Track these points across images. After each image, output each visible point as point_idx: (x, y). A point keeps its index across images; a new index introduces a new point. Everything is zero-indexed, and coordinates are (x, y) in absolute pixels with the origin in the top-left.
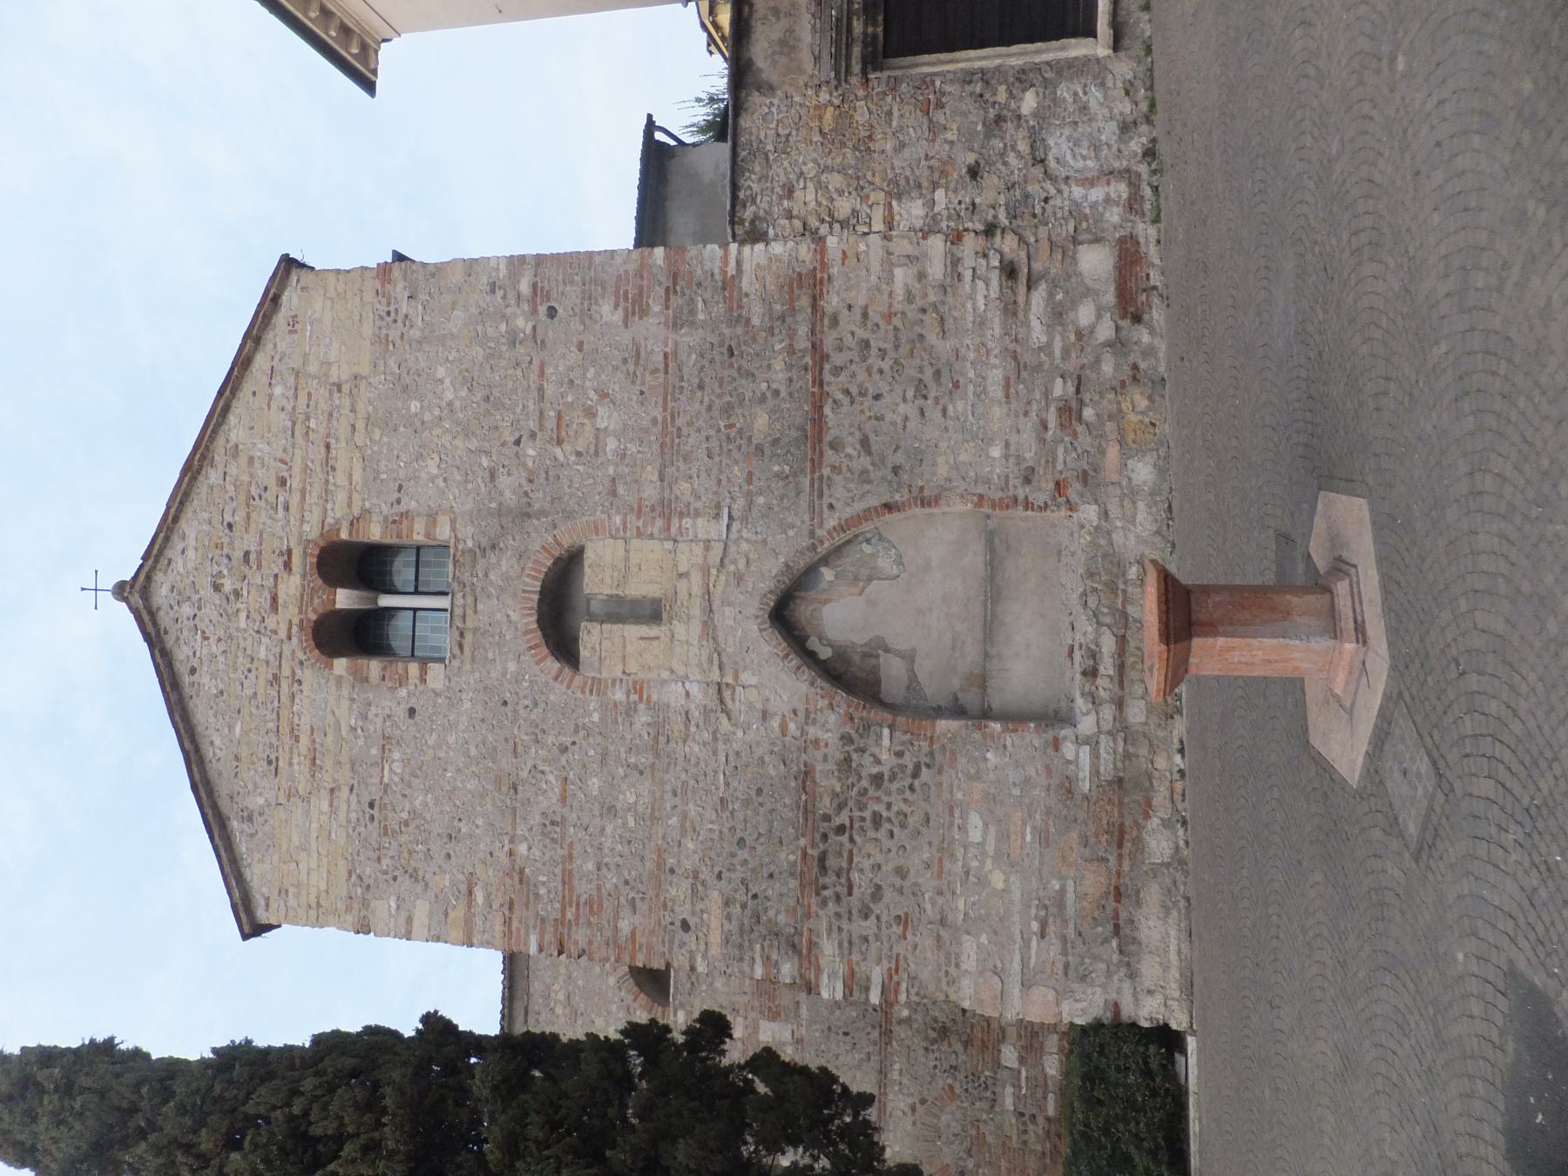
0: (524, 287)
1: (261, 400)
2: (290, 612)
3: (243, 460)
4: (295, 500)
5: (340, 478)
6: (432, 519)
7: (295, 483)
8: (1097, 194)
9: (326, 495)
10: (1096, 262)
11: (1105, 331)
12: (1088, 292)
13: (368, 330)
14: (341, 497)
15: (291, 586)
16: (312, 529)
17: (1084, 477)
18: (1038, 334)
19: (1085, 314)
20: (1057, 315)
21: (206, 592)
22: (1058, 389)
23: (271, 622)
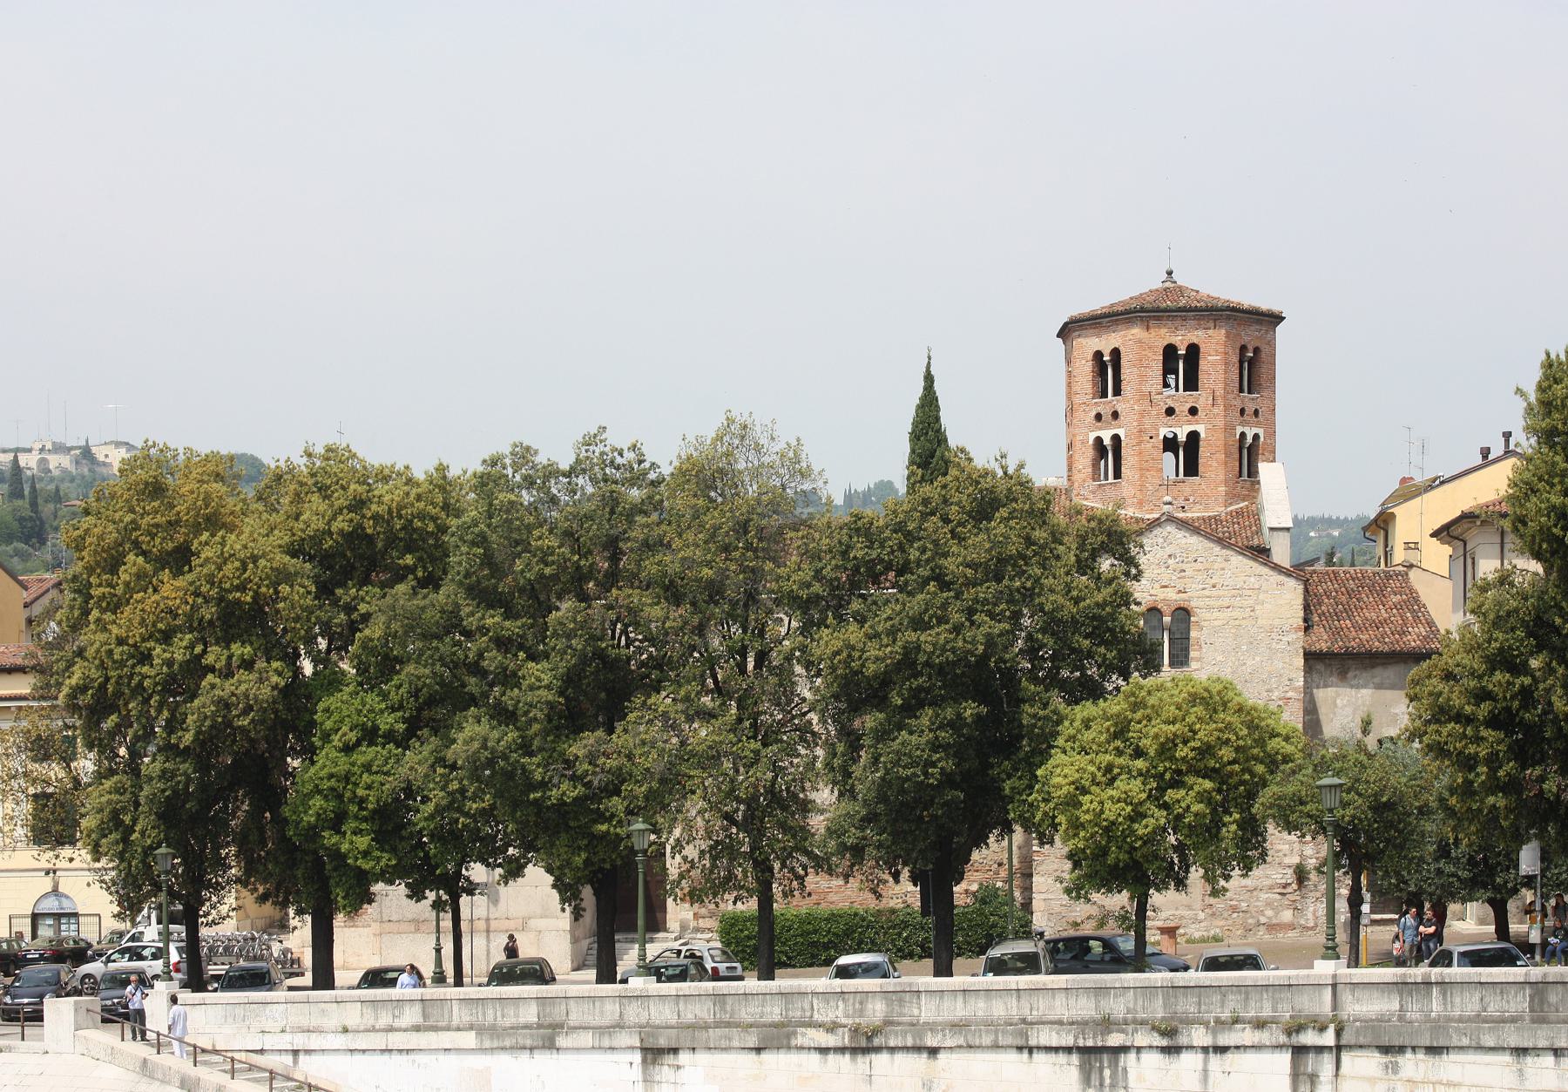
0: (1290, 694)
1: (1249, 571)
2: (1161, 594)
3: (1224, 565)
4: (1206, 592)
5: (1216, 614)
6: (1198, 660)
7: (1215, 592)
8: (1310, 916)
9: (1209, 608)
10: (1287, 916)
11: (1263, 920)
12: (1277, 914)
13: (1277, 622)
14: (1207, 616)
15: (1171, 595)
16: (1193, 604)
17: (1213, 914)
18: (1264, 896)
19: (1269, 913)
20: (1269, 904)
21: (1169, 550)
22: (1244, 905)
23: (1157, 585)
